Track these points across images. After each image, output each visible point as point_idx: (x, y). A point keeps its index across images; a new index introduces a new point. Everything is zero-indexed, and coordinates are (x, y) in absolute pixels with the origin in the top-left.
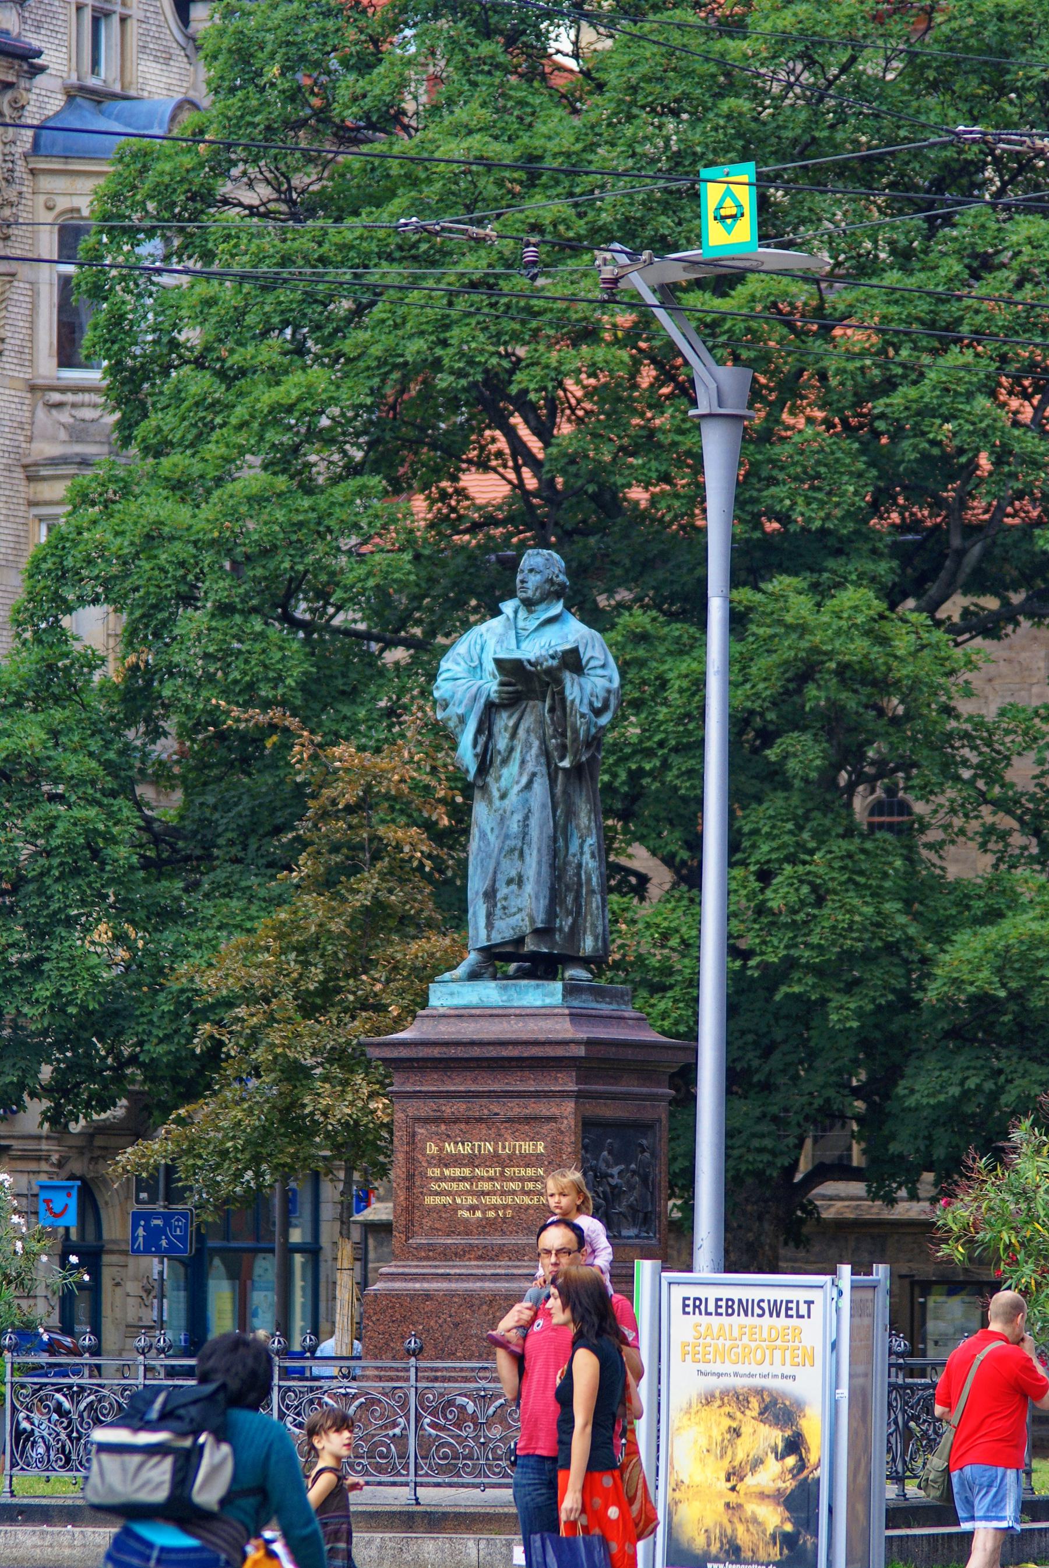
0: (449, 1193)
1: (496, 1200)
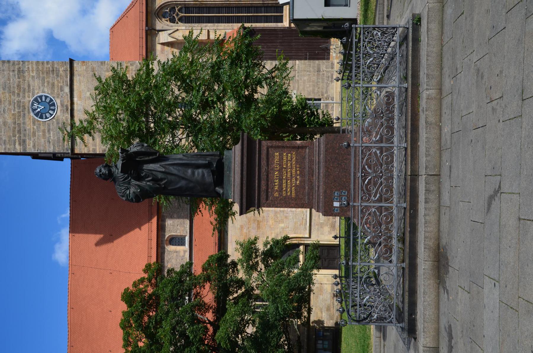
0: (291, 188)
1: (294, 171)
